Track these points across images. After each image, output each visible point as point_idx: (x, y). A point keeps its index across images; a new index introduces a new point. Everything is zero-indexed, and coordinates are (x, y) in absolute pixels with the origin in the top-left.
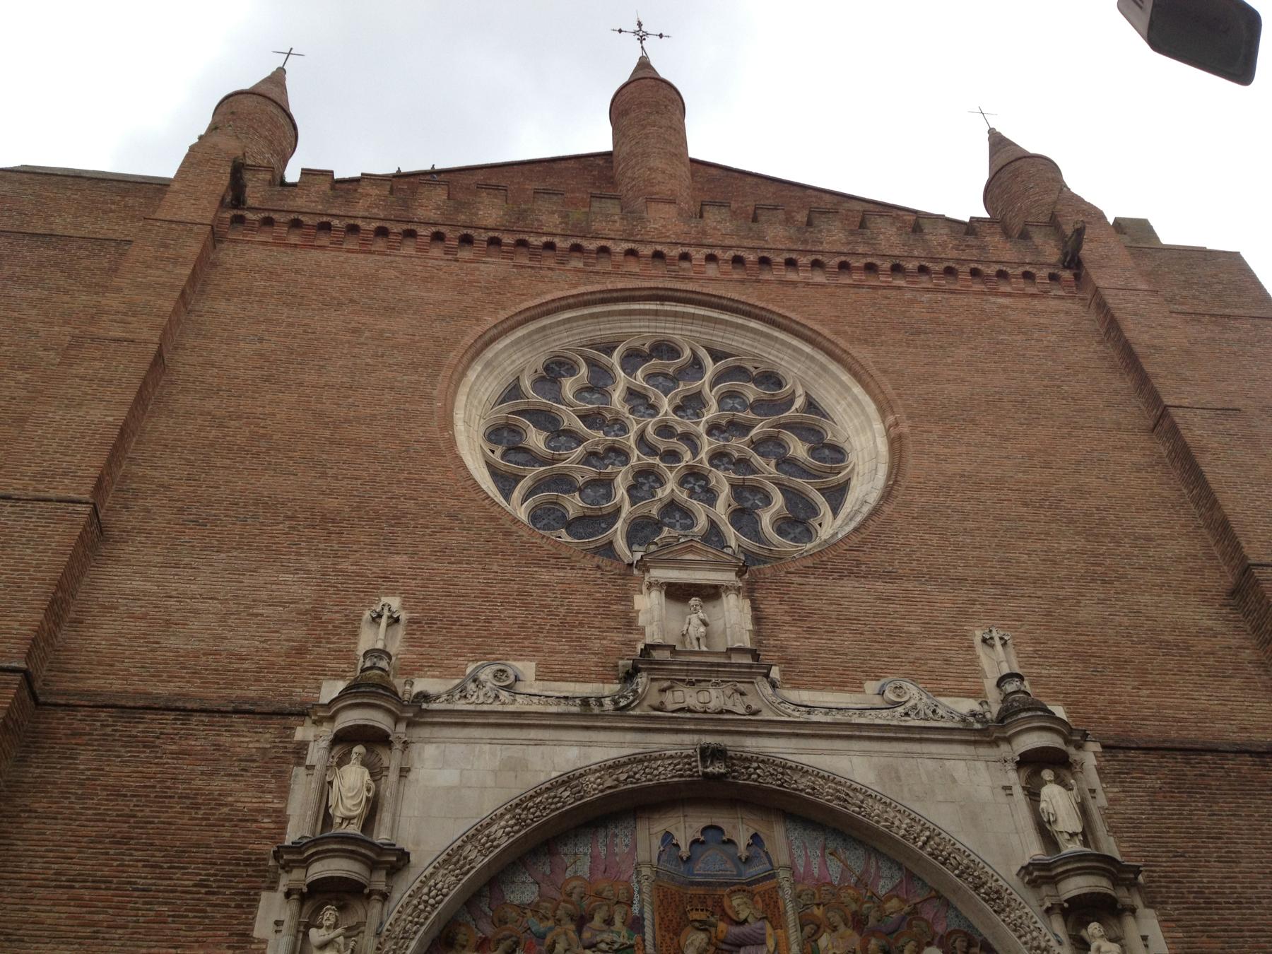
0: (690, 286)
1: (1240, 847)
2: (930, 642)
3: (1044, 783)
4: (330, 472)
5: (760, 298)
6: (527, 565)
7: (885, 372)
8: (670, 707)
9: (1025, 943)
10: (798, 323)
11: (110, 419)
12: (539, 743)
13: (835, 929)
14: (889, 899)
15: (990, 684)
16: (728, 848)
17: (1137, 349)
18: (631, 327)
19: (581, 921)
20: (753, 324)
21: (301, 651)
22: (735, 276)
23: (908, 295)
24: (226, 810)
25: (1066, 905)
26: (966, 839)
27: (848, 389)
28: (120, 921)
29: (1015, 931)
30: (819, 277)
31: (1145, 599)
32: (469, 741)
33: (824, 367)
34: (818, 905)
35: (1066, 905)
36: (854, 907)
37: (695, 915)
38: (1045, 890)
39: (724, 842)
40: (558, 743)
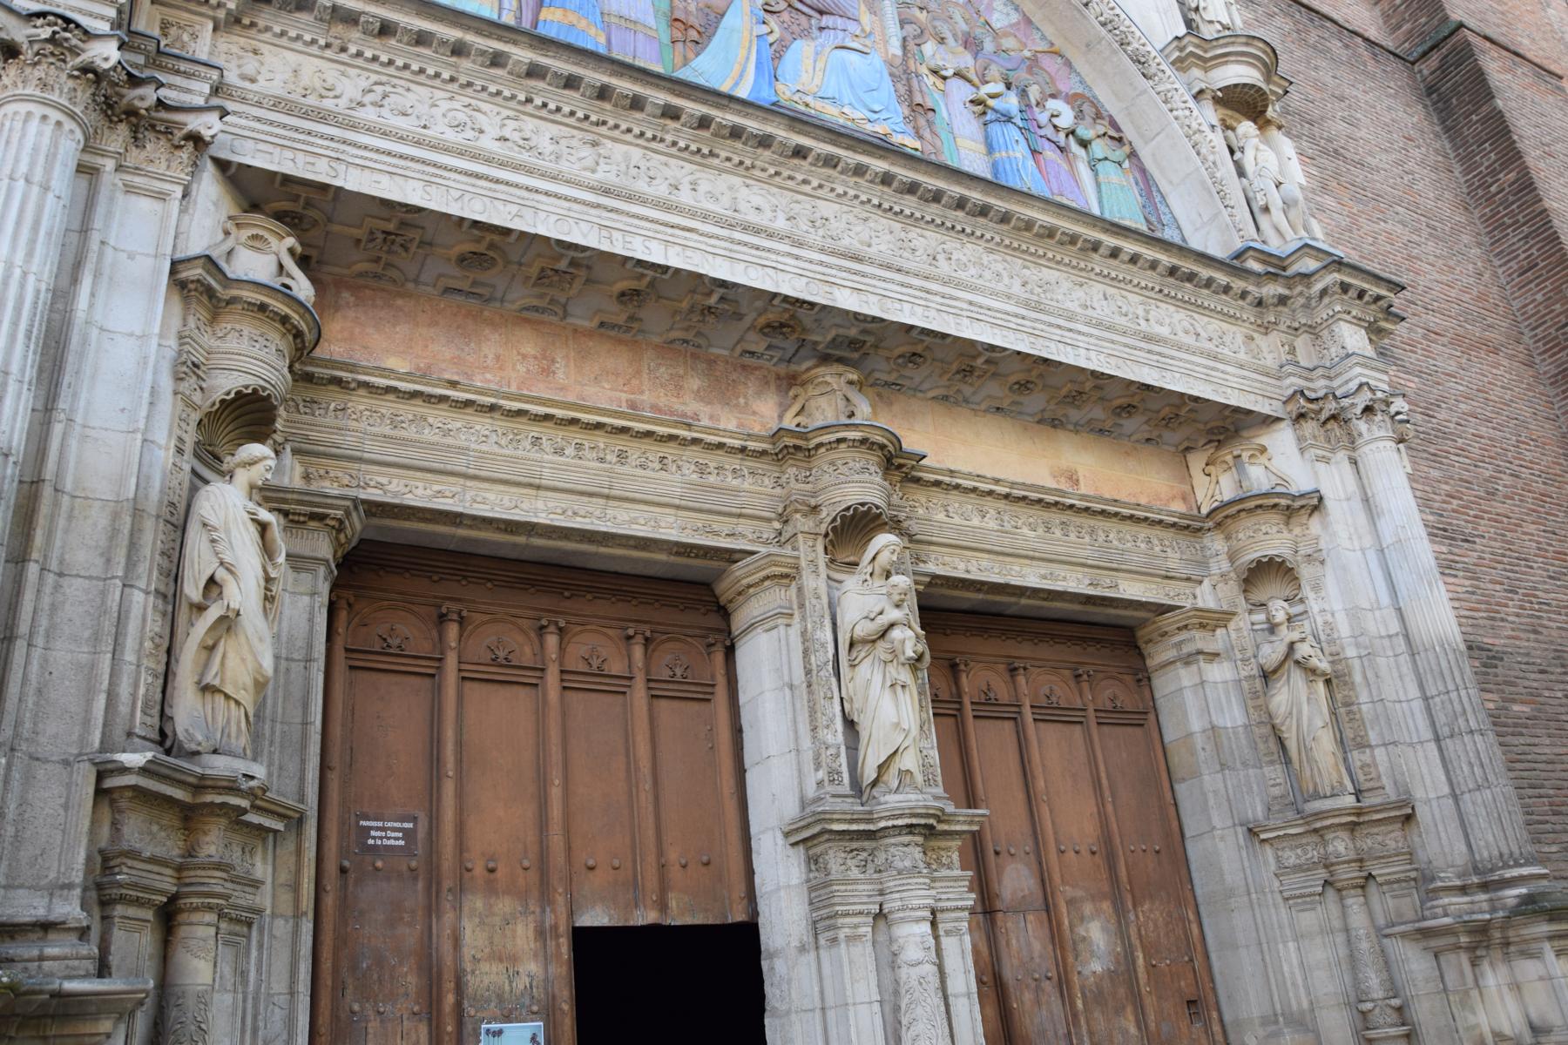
9: (1176, 118)
13: (942, 41)
14: (1006, 35)
25: (1220, 94)
29: (1166, 102)
34: (921, 8)
35: (1220, 94)
36: (965, 27)
38: (1196, 72)
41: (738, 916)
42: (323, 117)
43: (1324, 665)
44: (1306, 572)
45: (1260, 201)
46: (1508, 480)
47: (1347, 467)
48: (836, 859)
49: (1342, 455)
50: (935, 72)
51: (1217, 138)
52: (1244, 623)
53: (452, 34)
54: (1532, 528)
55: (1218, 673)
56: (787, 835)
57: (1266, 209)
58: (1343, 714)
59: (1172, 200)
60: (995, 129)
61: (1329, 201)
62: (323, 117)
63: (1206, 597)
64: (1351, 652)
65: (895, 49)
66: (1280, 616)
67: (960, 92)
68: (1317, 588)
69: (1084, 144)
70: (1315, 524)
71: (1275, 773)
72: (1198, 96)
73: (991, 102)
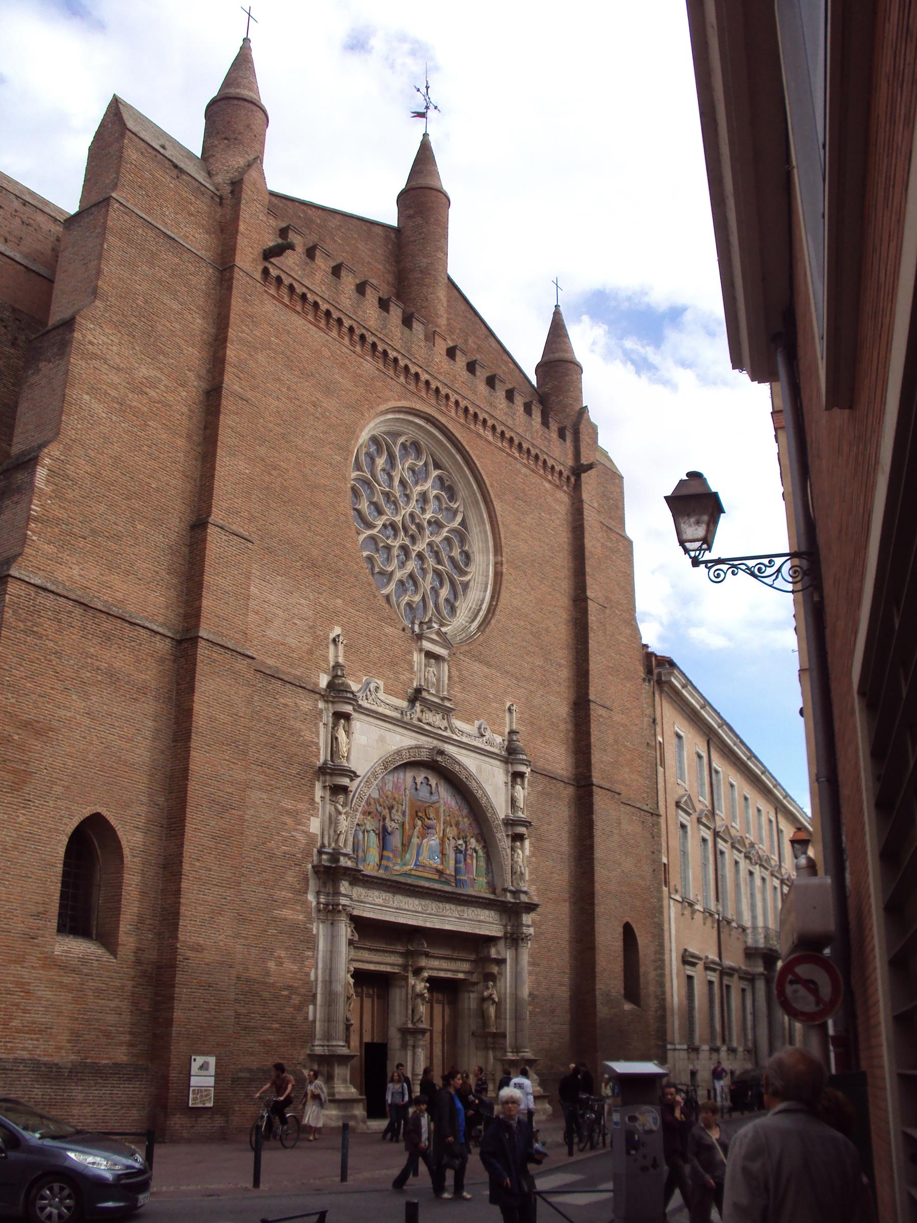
0: (443, 420)
1: (552, 820)
2: (495, 705)
3: (517, 784)
4: (313, 528)
5: (468, 442)
6: (381, 620)
7: (503, 524)
8: (424, 721)
10: (478, 470)
11: (247, 471)
12: (389, 730)
13: (451, 826)
15: (507, 730)
16: (429, 787)
17: (587, 554)
18: (407, 429)
19: (391, 808)
20: (458, 457)
21: (310, 652)
22: (462, 421)
23: (519, 466)
24: (302, 739)
26: (493, 800)
27: (484, 523)
28: (278, 785)
30: (489, 435)
31: (553, 699)
32: (370, 723)
33: (477, 502)
37: (420, 814)
39: (427, 784)
40: (395, 732)
41: (386, 1041)
42: (361, 902)
43: (496, 1000)
44: (498, 976)
45: (515, 870)
46: (555, 945)
47: (514, 951)
48: (409, 1037)
49: (514, 948)
50: (448, 839)
51: (509, 851)
52: (480, 987)
53: (380, 881)
54: (557, 959)
55: (472, 995)
56: (398, 1029)
57: (515, 873)
58: (498, 1011)
59: (493, 865)
60: (458, 855)
61: (534, 859)
62: (361, 902)
63: (474, 978)
64: (503, 997)
65: (441, 835)
66: (490, 986)
67: (453, 841)
68: (500, 980)
69: (476, 852)
70: (503, 966)
71: (480, 1020)
72: (507, 836)
73: (459, 847)
